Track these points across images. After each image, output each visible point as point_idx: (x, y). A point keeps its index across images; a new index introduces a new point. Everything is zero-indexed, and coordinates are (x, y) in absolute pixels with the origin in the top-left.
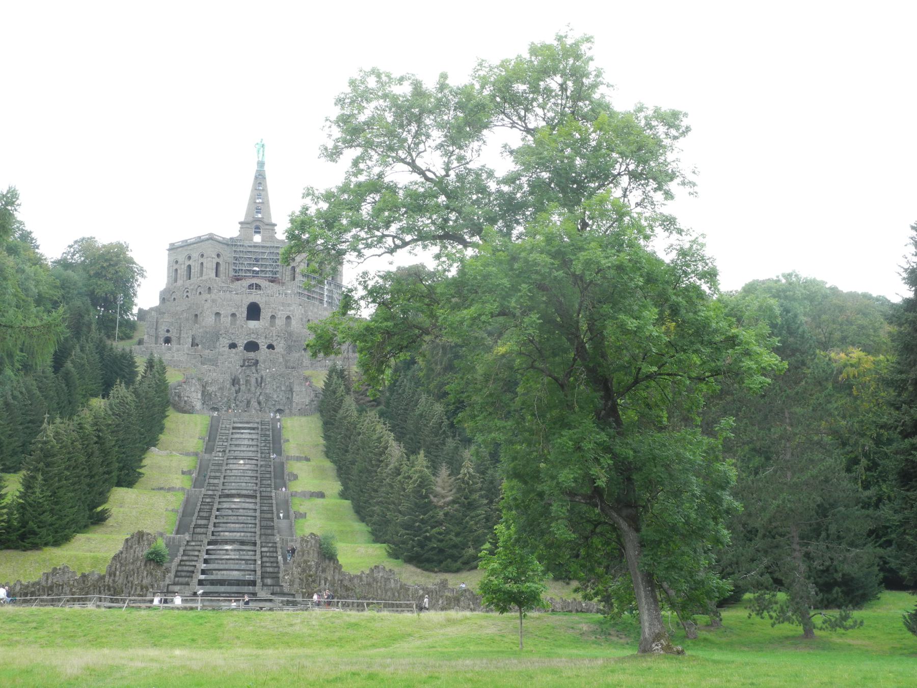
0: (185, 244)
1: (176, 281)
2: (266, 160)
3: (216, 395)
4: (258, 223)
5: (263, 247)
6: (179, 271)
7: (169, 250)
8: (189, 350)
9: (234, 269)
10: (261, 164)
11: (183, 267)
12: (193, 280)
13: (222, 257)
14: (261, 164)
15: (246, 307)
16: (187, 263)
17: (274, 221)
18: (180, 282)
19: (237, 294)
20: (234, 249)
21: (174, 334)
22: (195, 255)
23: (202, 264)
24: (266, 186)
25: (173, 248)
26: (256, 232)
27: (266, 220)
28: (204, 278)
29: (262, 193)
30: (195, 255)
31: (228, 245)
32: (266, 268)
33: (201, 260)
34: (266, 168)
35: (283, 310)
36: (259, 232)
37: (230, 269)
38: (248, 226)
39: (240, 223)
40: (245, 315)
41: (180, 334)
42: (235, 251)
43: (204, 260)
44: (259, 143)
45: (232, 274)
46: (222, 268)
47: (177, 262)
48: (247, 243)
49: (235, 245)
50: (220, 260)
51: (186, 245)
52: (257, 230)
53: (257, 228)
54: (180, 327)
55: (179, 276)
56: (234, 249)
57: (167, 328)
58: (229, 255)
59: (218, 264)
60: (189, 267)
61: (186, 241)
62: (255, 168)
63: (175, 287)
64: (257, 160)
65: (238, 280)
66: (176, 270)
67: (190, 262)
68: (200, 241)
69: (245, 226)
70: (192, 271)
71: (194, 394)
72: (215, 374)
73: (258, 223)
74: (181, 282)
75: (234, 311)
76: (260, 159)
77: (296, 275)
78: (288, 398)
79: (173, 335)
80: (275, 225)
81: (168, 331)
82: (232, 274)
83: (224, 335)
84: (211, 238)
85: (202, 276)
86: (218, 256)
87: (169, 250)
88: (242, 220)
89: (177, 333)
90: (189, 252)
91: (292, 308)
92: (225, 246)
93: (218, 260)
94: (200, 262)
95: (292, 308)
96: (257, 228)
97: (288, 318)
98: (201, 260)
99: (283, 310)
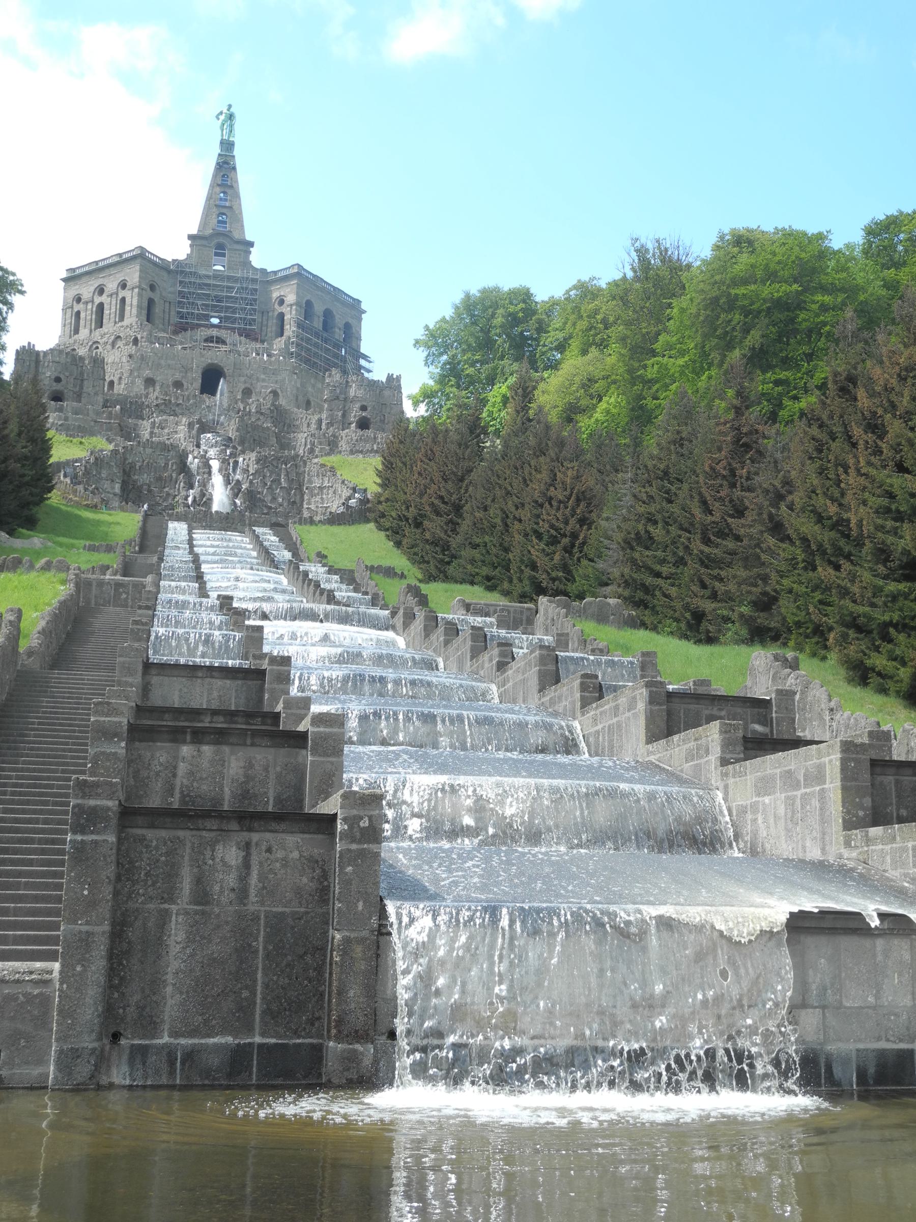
0: (93, 267)
1: (77, 331)
2: (238, 139)
3: (150, 491)
4: (221, 240)
5: (229, 278)
6: (82, 315)
7: (64, 280)
8: (98, 414)
9: (179, 313)
10: (227, 146)
11: (90, 306)
12: (109, 326)
13: (158, 291)
14: (227, 146)
15: (200, 372)
16: (97, 300)
17: (249, 237)
18: (84, 333)
19: (185, 349)
20: (180, 278)
21: (70, 387)
22: (111, 285)
23: (123, 300)
24: (237, 182)
25: (72, 278)
26: (216, 254)
27: (236, 235)
28: (127, 322)
29: (229, 191)
30: (111, 285)
31: (169, 272)
32: (234, 312)
33: (122, 294)
34: (237, 152)
35: (264, 380)
36: (224, 255)
37: (173, 313)
38: (204, 242)
39: (191, 237)
40: (198, 384)
41: (81, 387)
42: (181, 282)
43: (126, 293)
44: (225, 111)
45: (175, 319)
46: (157, 310)
47: (78, 300)
48: (203, 272)
49: (182, 272)
50: (156, 297)
51: (98, 269)
52: (220, 250)
53: (221, 246)
54: (82, 374)
55: (82, 322)
56: (180, 278)
57: (56, 374)
58: (170, 289)
59: (151, 302)
60: (101, 306)
61: (97, 262)
62: (217, 150)
63: (75, 342)
64: (219, 138)
65: (186, 330)
66: (78, 313)
67: (104, 299)
68: (122, 261)
69: (199, 242)
70: (106, 312)
71: (107, 485)
72: (150, 451)
73: (221, 240)
74: (87, 331)
75: (178, 376)
76: (225, 137)
77: (287, 327)
78: (294, 502)
79: (67, 386)
80: (251, 244)
81: (58, 380)
82: (175, 319)
83: (163, 407)
84: (141, 256)
85: (122, 318)
86: (152, 288)
87: (64, 280)
88: (194, 231)
89: (75, 386)
90: (100, 282)
91: (279, 378)
92: (165, 274)
93: (152, 295)
94: (120, 296)
95: (279, 378)
96: (221, 246)
97: (275, 393)
98: (122, 294)
99: (264, 380)
